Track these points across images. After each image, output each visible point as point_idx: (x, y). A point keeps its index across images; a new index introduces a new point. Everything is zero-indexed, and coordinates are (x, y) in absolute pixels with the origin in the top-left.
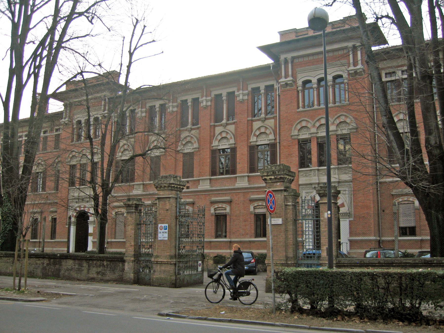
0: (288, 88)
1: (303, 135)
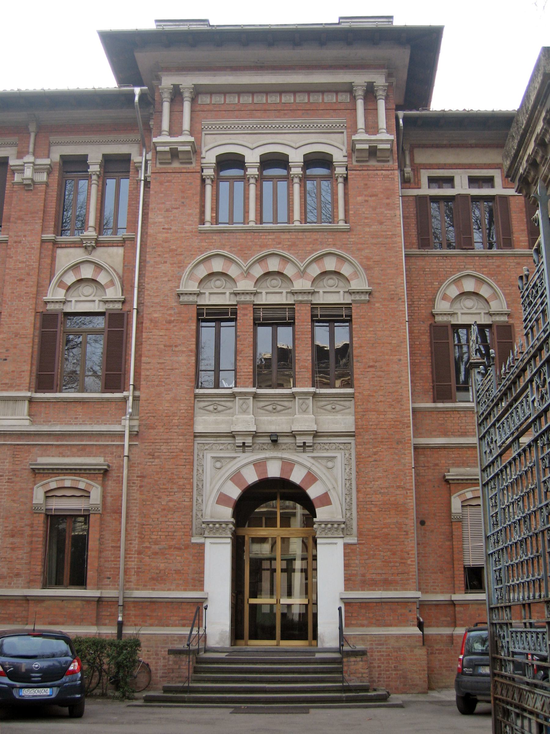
0: (176, 165)
1: (213, 296)
